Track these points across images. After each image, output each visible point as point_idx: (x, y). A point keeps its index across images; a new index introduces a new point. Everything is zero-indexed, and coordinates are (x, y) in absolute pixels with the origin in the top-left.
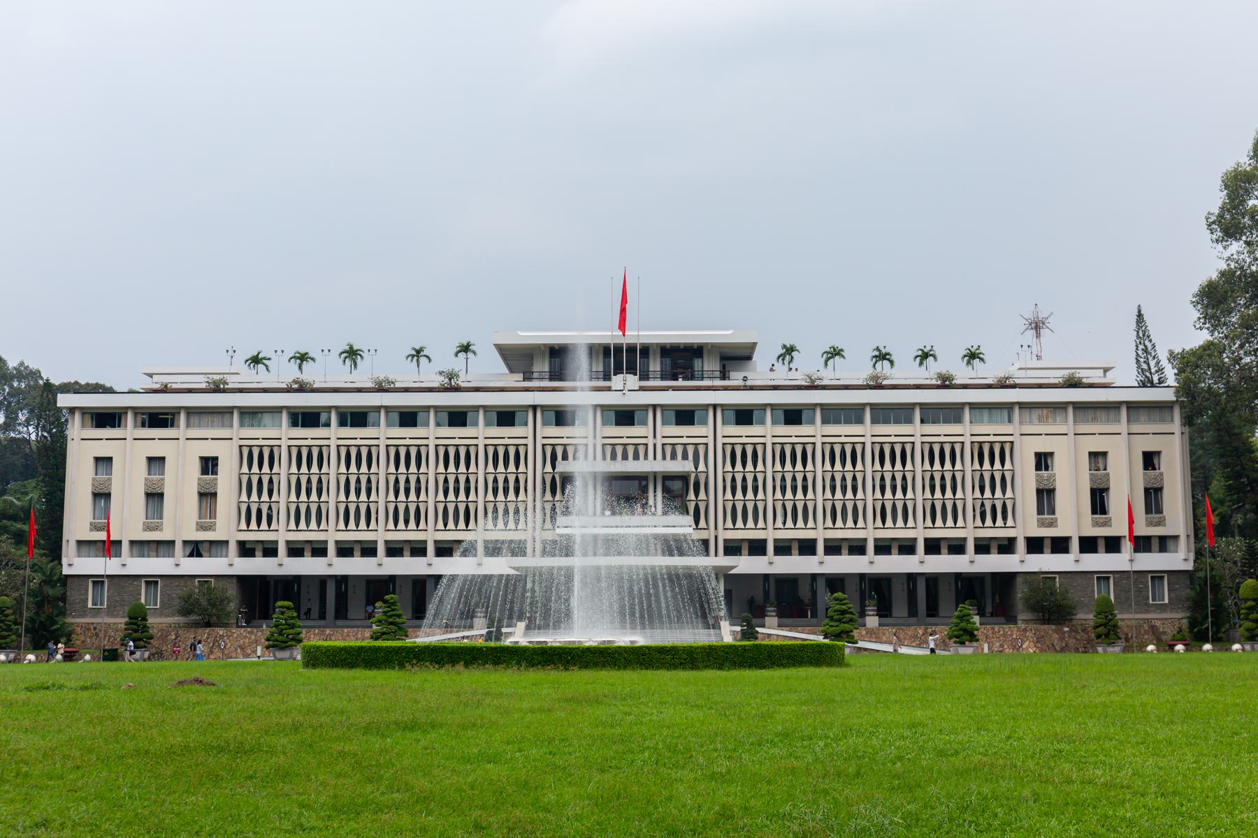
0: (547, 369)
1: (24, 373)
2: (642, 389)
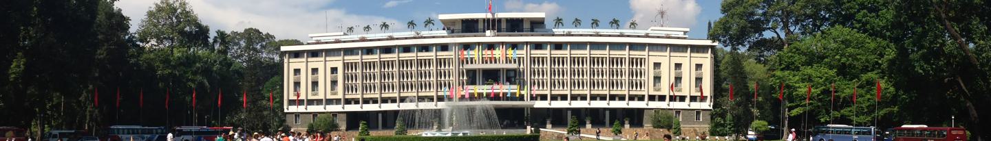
0: (460, 28)
1: (268, 35)
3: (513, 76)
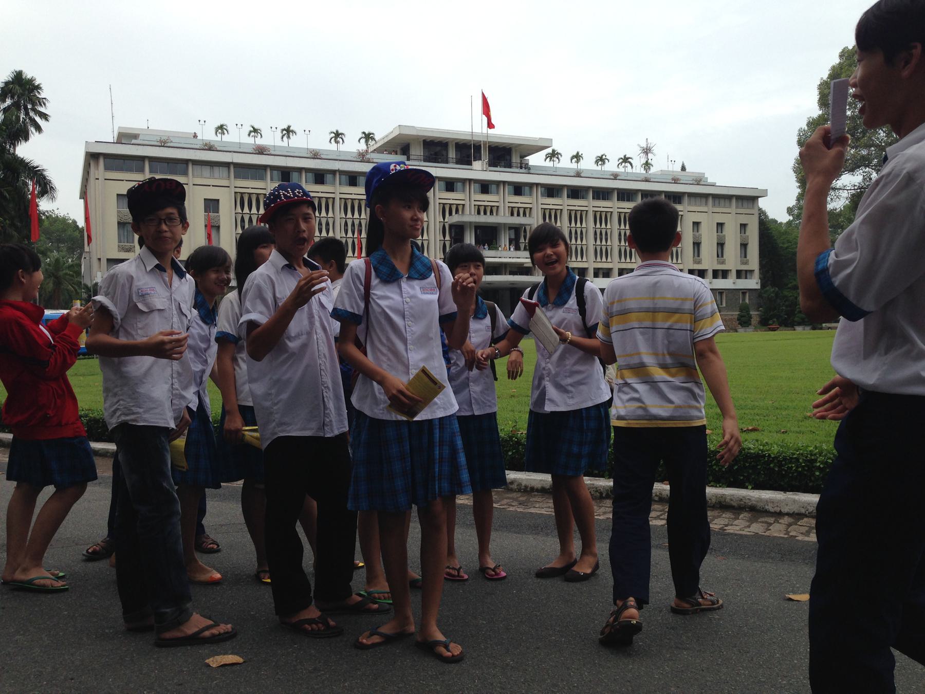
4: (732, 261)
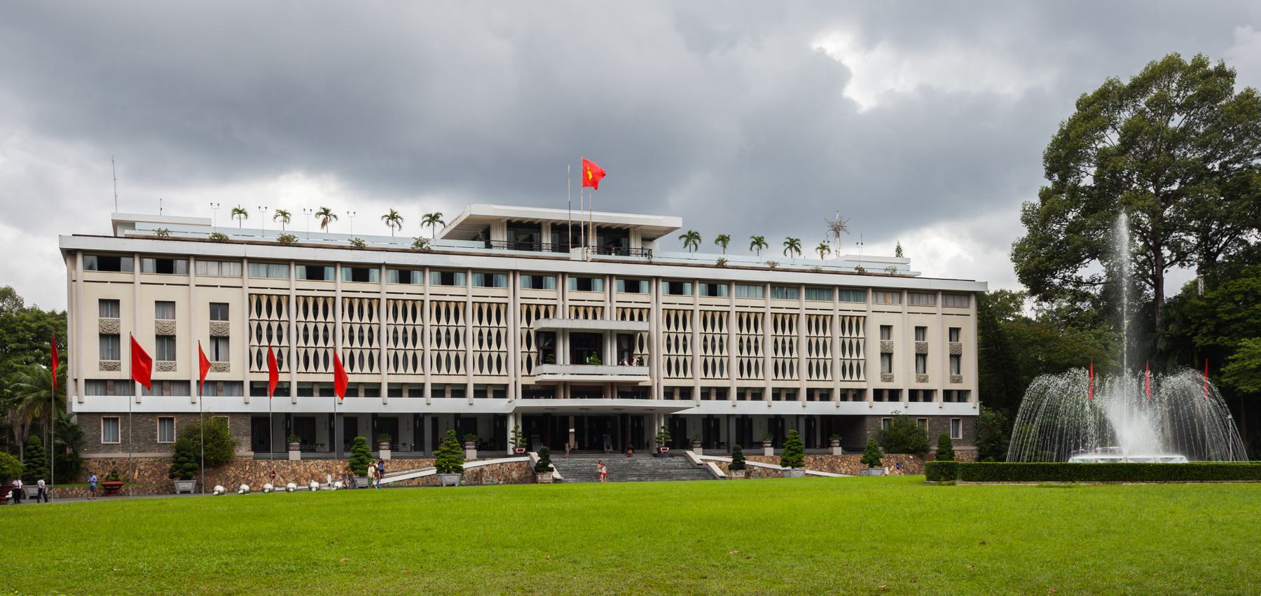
2: (593, 261)
3: (629, 344)
4: (938, 377)
